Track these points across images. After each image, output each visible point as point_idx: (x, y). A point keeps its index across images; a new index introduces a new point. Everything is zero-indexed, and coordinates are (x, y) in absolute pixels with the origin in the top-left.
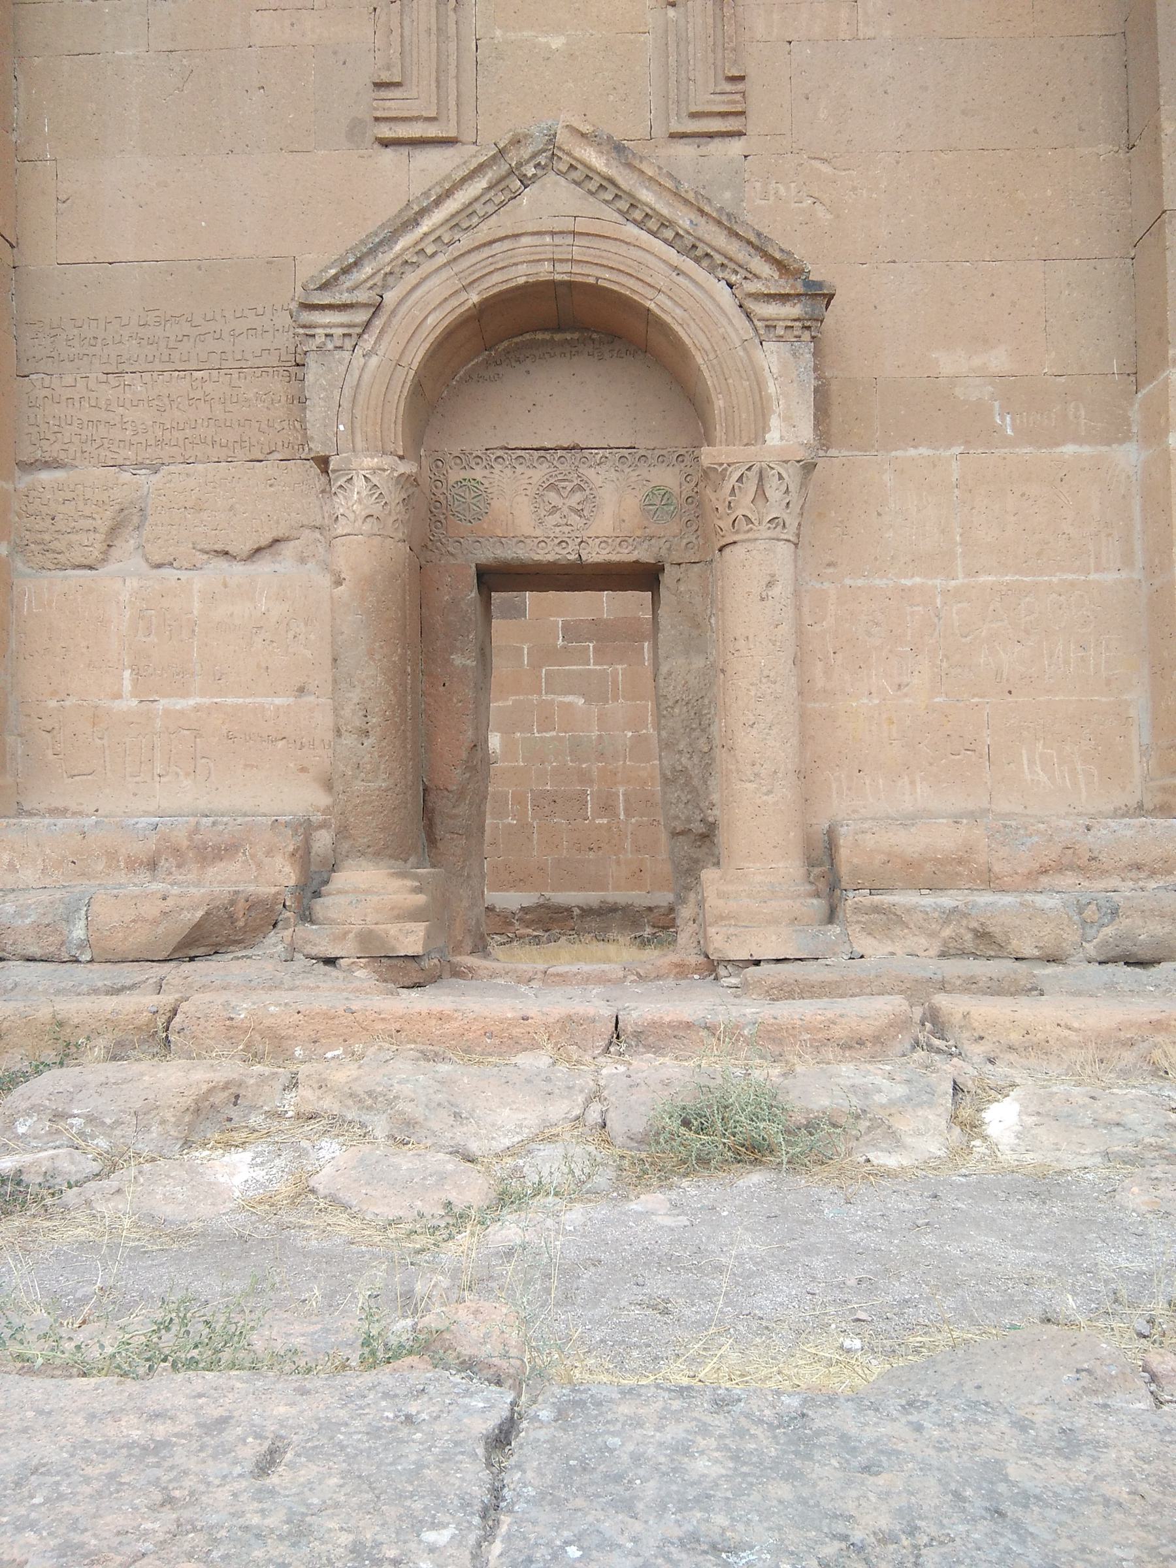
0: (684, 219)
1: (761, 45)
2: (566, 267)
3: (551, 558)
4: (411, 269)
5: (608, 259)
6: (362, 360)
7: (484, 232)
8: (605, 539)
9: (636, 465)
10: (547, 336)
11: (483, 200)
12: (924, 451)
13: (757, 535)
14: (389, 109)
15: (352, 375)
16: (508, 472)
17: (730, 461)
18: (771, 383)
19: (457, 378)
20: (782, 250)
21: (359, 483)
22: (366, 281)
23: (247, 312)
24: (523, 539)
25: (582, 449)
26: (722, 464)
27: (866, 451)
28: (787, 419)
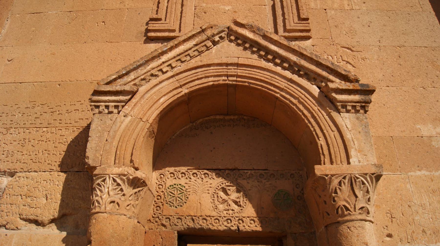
0: (294, 58)
1: (314, 10)
2: (235, 78)
3: (222, 228)
4: (154, 78)
5: (255, 75)
6: (123, 118)
7: (194, 63)
8: (252, 218)
9: (269, 179)
10: (222, 117)
11: (193, 49)
12: (424, 172)
13: (353, 217)
14: (155, 27)
15: (116, 125)
16: (199, 181)
17: (332, 173)
18: (348, 134)
19: (175, 135)
20: (345, 70)
21: (109, 182)
22: (130, 82)
23: (76, 103)
24: (205, 217)
25: (239, 170)
26: (327, 175)
27: (394, 172)
28: (360, 151)
